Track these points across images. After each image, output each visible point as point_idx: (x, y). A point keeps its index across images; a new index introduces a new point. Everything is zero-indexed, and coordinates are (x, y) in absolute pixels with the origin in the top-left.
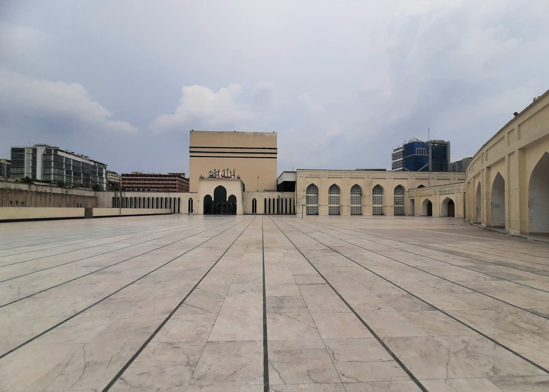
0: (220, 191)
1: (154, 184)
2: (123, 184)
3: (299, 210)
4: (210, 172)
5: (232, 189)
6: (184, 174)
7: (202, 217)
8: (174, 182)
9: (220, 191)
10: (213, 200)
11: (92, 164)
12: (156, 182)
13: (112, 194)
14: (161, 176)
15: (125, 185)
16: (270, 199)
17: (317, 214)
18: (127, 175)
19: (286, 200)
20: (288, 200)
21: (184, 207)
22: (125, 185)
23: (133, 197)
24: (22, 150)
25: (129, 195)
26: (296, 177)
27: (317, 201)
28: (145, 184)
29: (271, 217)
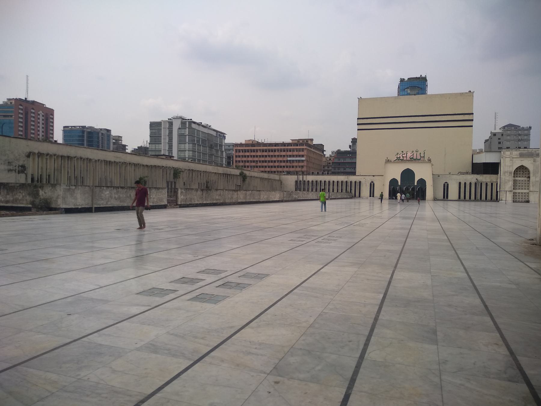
0: (408, 174)
1: (275, 156)
2: (236, 156)
3: (502, 196)
4: (398, 154)
5: (421, 172)
6: (312, 140)
7: (386, 201)
8: (301, 153)
9: (408, 174)
10: (399, 184)
11: (214, 134)
12: (277, 153)
13: (294, 178)
14: (284, 144)
15: (238, 159)
16: (465, 183)
17: (528, 202)
18: (241, 145)
19: (487, 184)
20: (489, 184)
21: (365, 191)
22: (238, 159)
23: (314, 181)
24: (158, 124)
25: (310, 178)
26: (501, 157)
27: (529, 186)
28: (263, 156)
29: (467, 203)
